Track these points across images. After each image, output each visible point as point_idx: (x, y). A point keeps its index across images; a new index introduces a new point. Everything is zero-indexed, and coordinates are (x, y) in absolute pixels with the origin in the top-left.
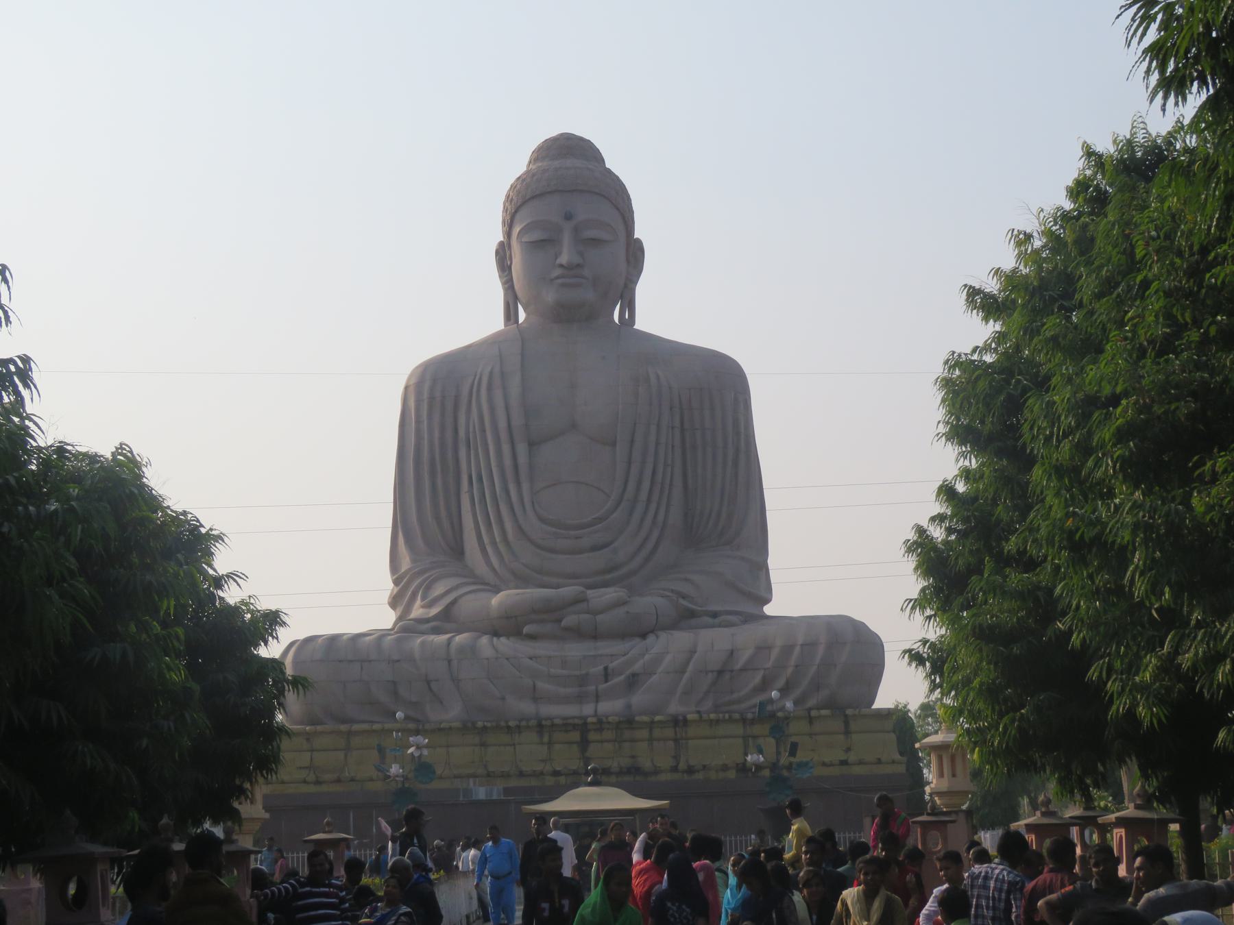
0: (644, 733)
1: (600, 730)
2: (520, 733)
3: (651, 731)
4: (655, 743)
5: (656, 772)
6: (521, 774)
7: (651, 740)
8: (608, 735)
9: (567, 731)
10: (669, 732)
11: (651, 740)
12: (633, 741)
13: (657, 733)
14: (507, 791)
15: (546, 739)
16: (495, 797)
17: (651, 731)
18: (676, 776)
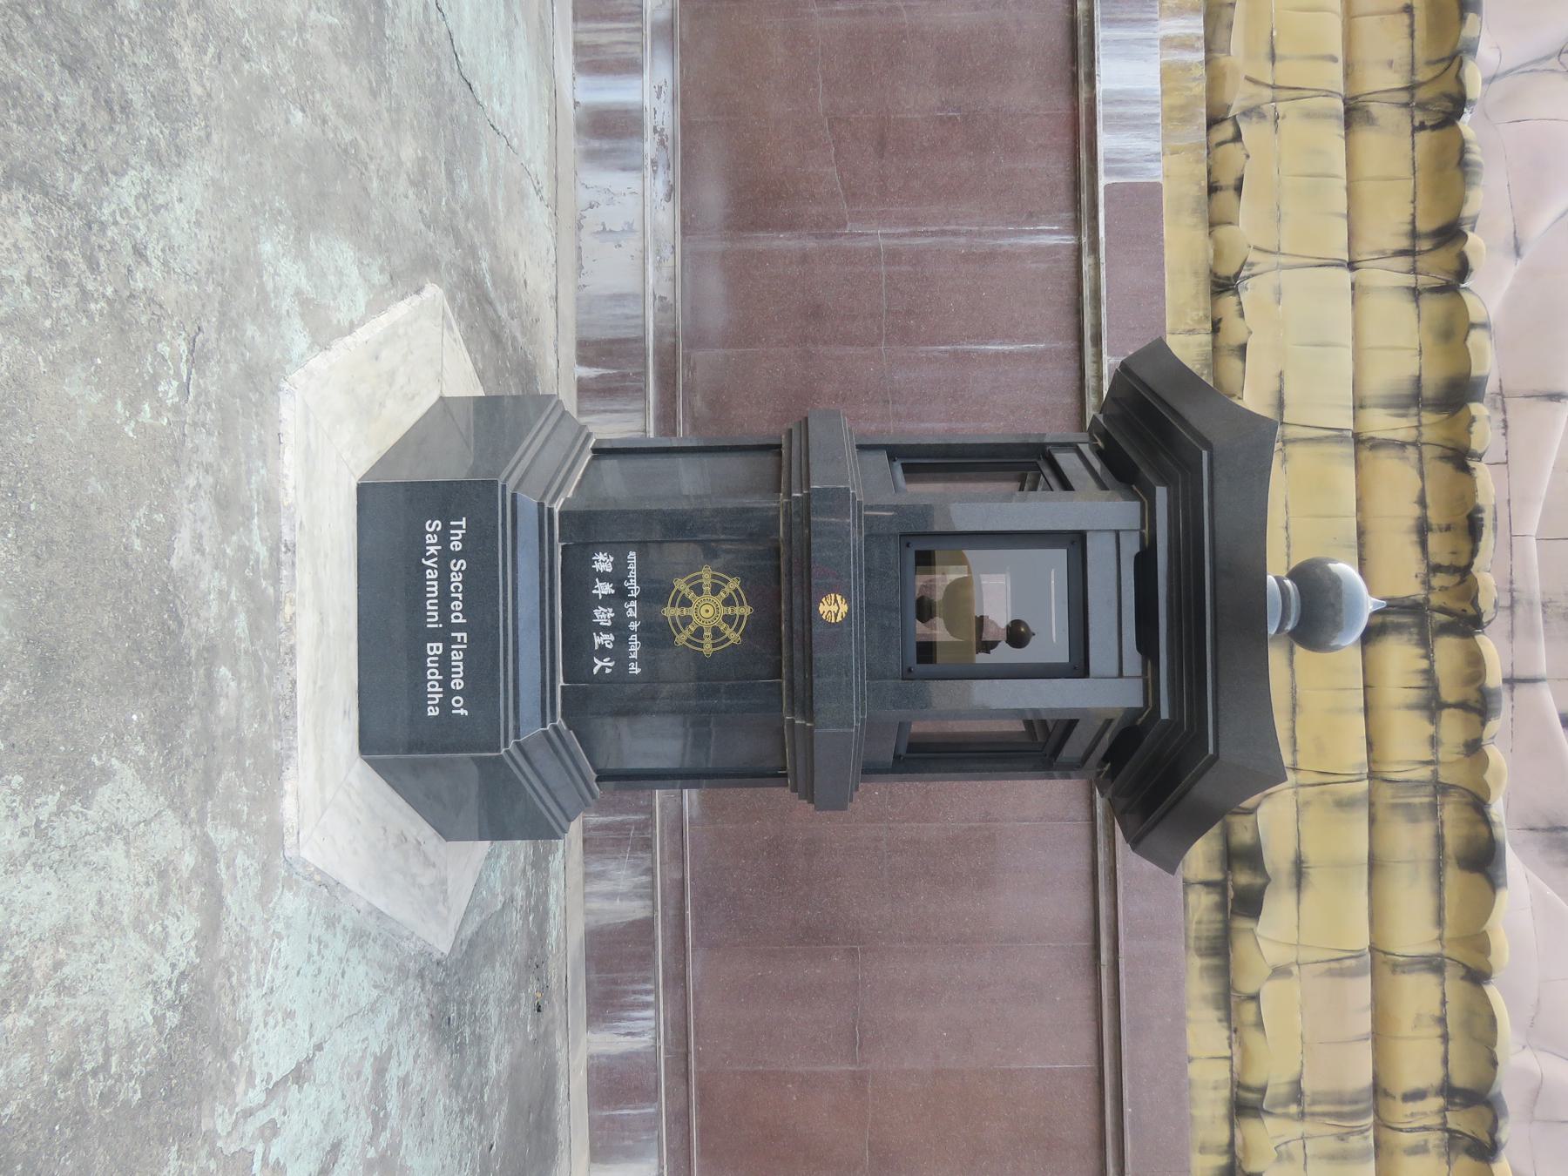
0: (1413, 932)
1: (1432, 705)
2: (1415, 293)
3: (1435, 965)
4: (1362, 988)
5: (1231, 1001)
6: (1222, 285)
7: (1380, 962)
8: (1408, 742)
9: (1423, 530)
10: (1419, 1062)
11: (1380, 962)
12: (1374, 864)
13: (1418, 996)
14: (1143, 202)
15: (1381, 423)
16: (1106, 142)
17: (1435, 965)
18: (1209, 1109)
